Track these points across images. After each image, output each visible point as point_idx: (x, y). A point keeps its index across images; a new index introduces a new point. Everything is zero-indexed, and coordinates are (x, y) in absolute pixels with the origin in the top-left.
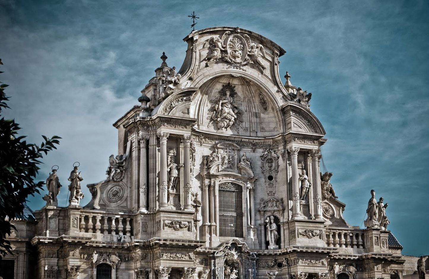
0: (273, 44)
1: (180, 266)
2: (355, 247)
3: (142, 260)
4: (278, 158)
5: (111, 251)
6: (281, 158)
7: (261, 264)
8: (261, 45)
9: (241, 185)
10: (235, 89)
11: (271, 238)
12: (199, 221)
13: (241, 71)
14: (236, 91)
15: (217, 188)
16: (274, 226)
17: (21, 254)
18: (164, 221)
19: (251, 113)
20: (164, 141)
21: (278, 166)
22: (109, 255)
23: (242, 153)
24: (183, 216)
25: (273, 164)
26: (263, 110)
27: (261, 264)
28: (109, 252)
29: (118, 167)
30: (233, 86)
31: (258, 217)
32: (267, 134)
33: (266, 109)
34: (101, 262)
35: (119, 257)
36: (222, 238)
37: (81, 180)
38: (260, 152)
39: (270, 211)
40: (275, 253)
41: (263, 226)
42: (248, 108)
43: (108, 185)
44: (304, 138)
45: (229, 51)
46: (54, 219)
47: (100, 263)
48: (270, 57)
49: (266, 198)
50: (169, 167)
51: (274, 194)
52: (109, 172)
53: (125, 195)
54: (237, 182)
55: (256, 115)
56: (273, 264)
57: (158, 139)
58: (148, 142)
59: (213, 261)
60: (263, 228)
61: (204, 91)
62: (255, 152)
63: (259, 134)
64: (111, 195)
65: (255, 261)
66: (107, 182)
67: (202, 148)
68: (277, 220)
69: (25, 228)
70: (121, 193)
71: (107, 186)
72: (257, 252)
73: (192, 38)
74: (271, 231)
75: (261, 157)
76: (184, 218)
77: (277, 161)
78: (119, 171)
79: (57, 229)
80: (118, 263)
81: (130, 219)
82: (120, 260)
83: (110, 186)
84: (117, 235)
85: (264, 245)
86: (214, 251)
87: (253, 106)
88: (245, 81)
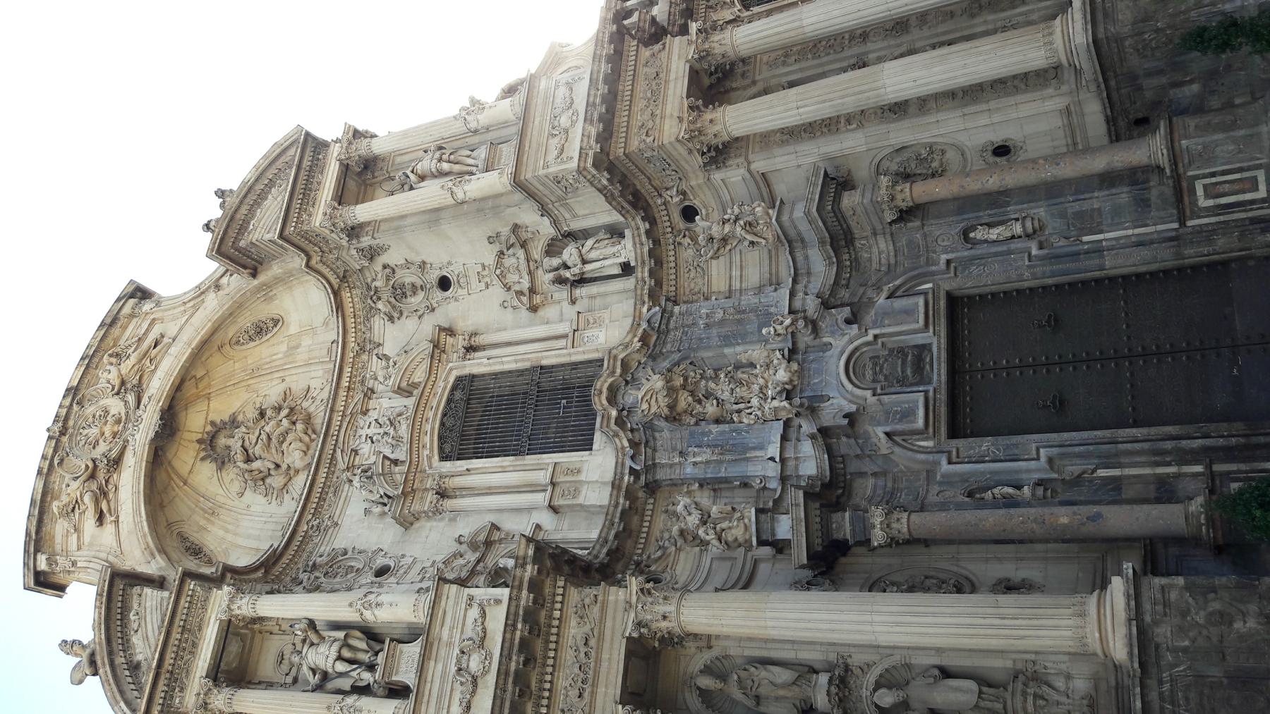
0: (109, 321)
4: (385, 267)
6: (383, 259)
7: (692, 285)
8: (106, 356)
9: (452, 379)
10: (218, 422)
11: (608, 256)
12: (538, 527)
13: (148, 408)
14: (226, 418)
15: (448, 466)
16: (570, 253)
19: (285, 364)
21: (408, 264)
24: (445, 634)
25: (408, 278)
26: (280, 323)
27: (692, 285)
30: (209, 428)
31: (549, 312)
33: (276, 322)
36: (598, 436)
39: (530, 273)
40: (644, 238)
41: (578, 292)
42: (277, 375)
48: (143, 325)
51: (484, 267)
54: (442, 395)
55: (293, 348)
56: (687, 240)
59: (661, 475)
60: (579, 292)
61: (203, 522)
62: (381, 342)
65: (677, 309)
72: (644, 303)
73: (37, 574)
74: (584, 262)
75: (391, 319)
76: (451, 629)
77: (396, 268)
85: (629, 283)
86: (627, 471)
87: (268, 360)
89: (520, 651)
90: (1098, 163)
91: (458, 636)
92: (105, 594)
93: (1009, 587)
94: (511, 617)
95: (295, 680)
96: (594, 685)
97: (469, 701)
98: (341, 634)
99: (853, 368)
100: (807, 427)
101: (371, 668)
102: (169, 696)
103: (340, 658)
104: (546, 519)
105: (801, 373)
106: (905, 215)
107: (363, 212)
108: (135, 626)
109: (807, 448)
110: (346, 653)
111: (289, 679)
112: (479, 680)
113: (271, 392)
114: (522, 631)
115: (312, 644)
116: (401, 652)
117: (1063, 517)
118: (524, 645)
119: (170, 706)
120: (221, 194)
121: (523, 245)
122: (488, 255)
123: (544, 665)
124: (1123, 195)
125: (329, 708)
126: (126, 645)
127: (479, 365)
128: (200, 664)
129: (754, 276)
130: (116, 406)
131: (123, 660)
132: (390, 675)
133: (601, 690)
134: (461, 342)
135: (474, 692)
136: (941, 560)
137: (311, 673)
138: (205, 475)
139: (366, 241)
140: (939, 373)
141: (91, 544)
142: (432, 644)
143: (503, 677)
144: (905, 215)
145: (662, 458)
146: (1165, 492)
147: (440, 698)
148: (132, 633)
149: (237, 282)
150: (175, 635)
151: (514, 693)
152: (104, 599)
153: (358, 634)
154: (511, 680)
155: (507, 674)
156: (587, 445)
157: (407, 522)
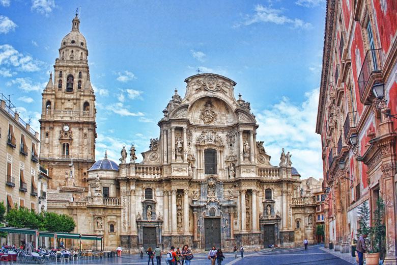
1: (182, 188)
2: (275, 176)
11: (231, 173)
15: (203, 151)
16: (233, 168)
20: (173, 130)
23: (216, 134)
31: (225, 164)
32: (229, 124)
36: (206, 175)
37: (135, 151)
38: (226, 133)
44: (246, 124)
45: (207, 85)
49: (229, 155)
52: (150, 147)
55: (224, 115)
57: (171, 129)
58: (167, 131)
63: (226, 125)
66: (150, 151)
67: (196, 133)
68: (234, 165)
83: (151, 153)
88: (218, 100)
90: (232, 233)
93: (190, 224)
99: (213, 208)
100: (206, 204)
104: (196, 168)
105: (213, 202)
106: (230, 214)
107: (241, 137)
109: (204, 204)
113: (217, 112)
117: (196, 229)
120: (249, 104)
121: (234, 161)
122: (233, 154)
124: (229, 235)
127: (218, 154)
129: (226, 194)
130: (215, 86)
134: (222, 150)
136: (192, 218)
138: (204, 103)
139: (238, 134)
140: (212, 217)
141: (192, 88)
144: (230, 214)
145: (203, 185)
146: (198, 237)
149: (234, 107)
156: (205, 174)
157: (196, 146)
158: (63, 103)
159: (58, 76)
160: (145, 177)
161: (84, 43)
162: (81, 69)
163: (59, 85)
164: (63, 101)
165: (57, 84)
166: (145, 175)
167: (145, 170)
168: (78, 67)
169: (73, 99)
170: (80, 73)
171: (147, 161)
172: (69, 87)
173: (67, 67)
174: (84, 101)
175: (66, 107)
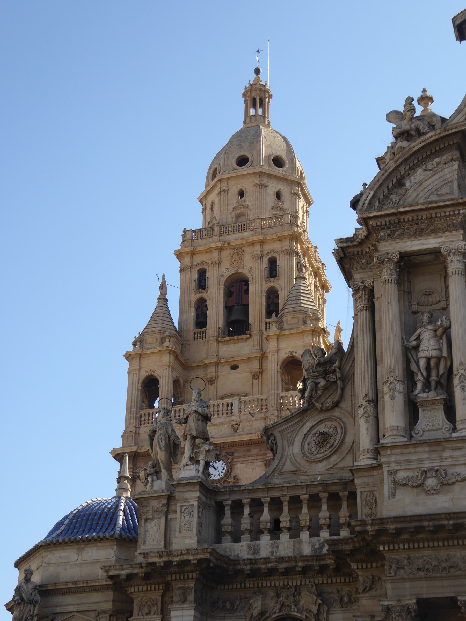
3: (364, 591)
5: (297, 581)
17: (103, 617)
18: (391, 473)
22: (297, 591)
24: (447, 453)
28: (295, 584)
29: (325, 375)
34: (275, 613)
35: (319, 595)
43: (305, 423)
46: (156, 520)
47: (274, 616)
50: (413, 338)
53: (349, 440)
58: (372, 291)
64: (313, 445)
69: (112, 555)
70: (339, 436)
71: (301, 424)
76: (451, 457)
78: (322, 382)
79: (163, 543)
80: (318, 610)
81: (346, 493)
82: (320, 602)
83: (309, 425)
84: (314, 539)
89: (435, 526)
91: (447, 463)
92: (446, 133)
94: (455, 515)
95: (415, 313)
96: (427, 578)
97: (407, 485)
98: (445, 354)
101: (427, 386)
102: (383, 227)
103: (428, 360)
108: (429, 167)
110: (433, 363)
111: (415, 308)
112: (420, 489)
114: (448, 524)
115: (435, 331)
116: (438, 409)
118: (439, 528)
119: (378, 230)
123: (433, 540)
125: (391, 372)
126: (413, 169)
128: (409, 243)
131: (403, 172)
132: (422, 406)
133: (424, 584)
135: (413, 487)
137: (416, 337)
142: (439, 445)
143: (418, 519)
147: (405, 461)
148: (424, 167)
150: (424, 215)
151: (410, 528)
152: (443, 134)
153: (449, 364)
154: (417, 524)
155: (420, 520)
158: (212, 381)
159: (194, 285)
160: (264, 553)
161: (283, 154)
162: (276, 246)
163: (197, 316)
164: (211, 372)
165: (192, 314)
166: (265, 539)
167: (266, 515)
168: (262, 243)
169: (249, 359)
170: (273, 263)
171: (288, 467)
172: (235, 317)
173: (221, 249)
174: (283, 355)
175: (220, 393)
